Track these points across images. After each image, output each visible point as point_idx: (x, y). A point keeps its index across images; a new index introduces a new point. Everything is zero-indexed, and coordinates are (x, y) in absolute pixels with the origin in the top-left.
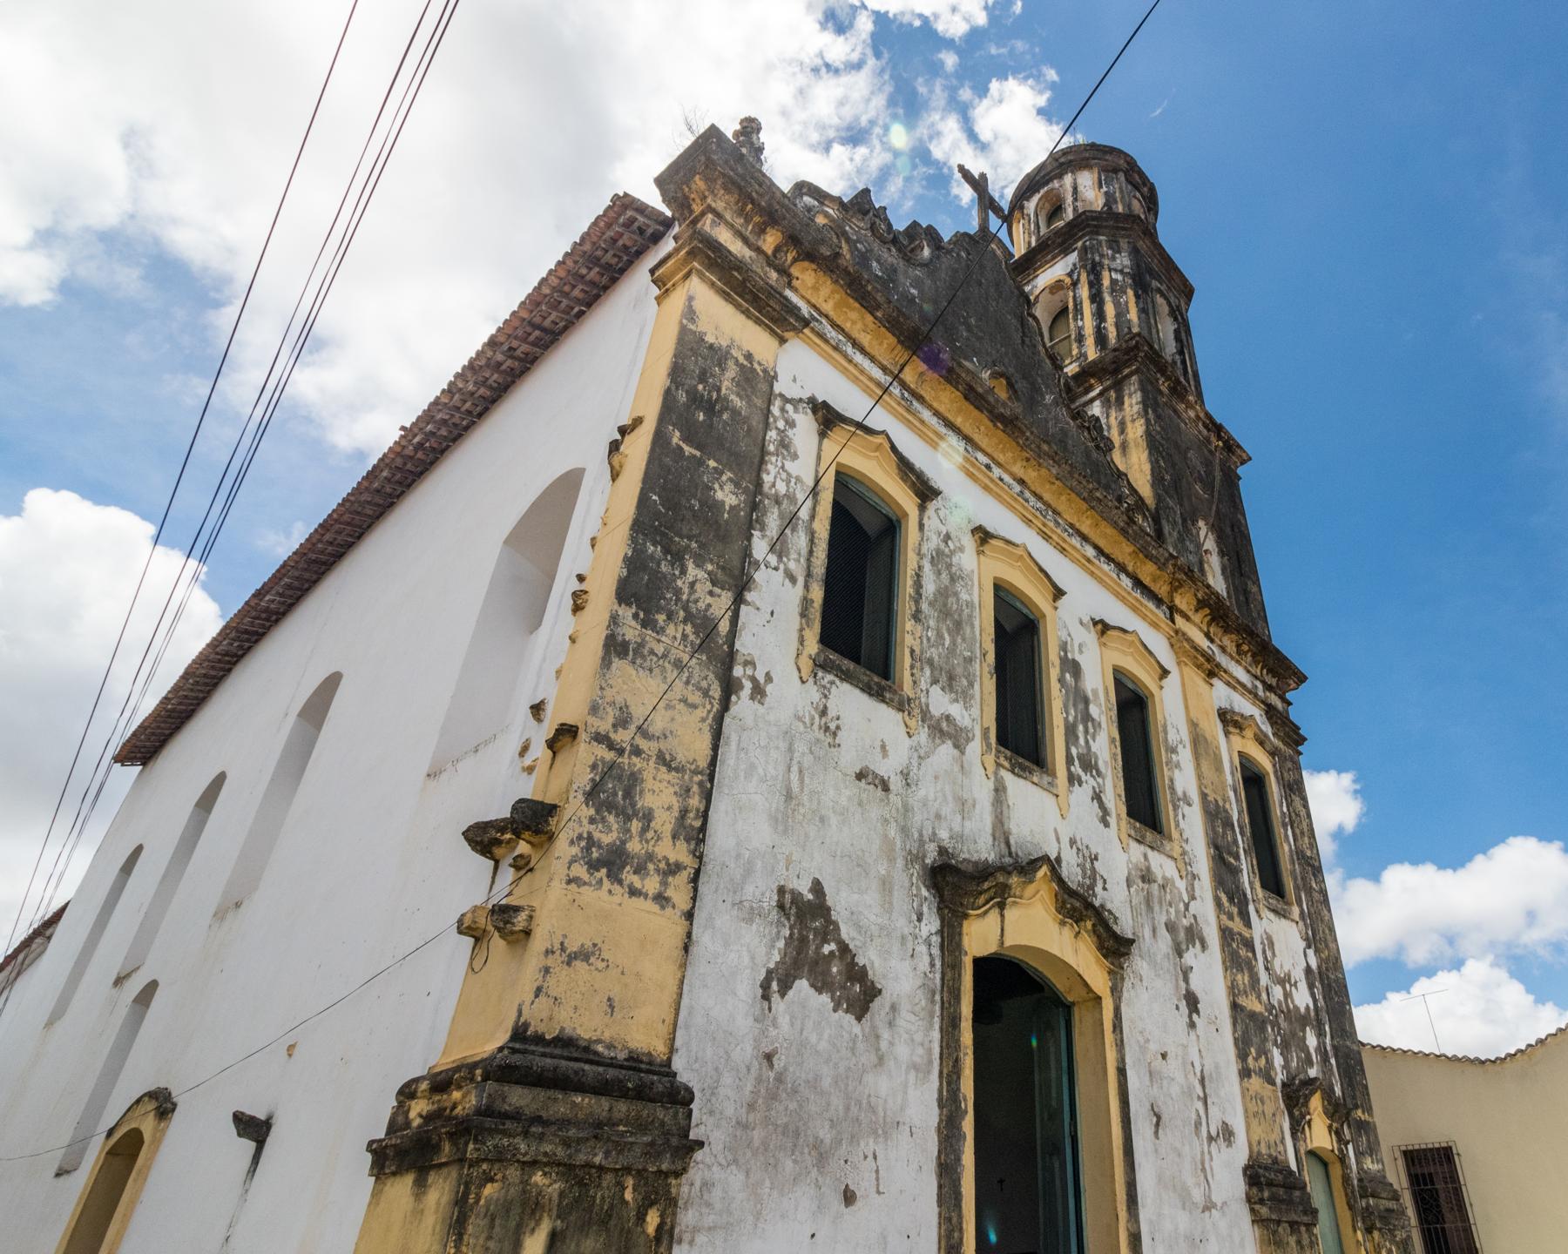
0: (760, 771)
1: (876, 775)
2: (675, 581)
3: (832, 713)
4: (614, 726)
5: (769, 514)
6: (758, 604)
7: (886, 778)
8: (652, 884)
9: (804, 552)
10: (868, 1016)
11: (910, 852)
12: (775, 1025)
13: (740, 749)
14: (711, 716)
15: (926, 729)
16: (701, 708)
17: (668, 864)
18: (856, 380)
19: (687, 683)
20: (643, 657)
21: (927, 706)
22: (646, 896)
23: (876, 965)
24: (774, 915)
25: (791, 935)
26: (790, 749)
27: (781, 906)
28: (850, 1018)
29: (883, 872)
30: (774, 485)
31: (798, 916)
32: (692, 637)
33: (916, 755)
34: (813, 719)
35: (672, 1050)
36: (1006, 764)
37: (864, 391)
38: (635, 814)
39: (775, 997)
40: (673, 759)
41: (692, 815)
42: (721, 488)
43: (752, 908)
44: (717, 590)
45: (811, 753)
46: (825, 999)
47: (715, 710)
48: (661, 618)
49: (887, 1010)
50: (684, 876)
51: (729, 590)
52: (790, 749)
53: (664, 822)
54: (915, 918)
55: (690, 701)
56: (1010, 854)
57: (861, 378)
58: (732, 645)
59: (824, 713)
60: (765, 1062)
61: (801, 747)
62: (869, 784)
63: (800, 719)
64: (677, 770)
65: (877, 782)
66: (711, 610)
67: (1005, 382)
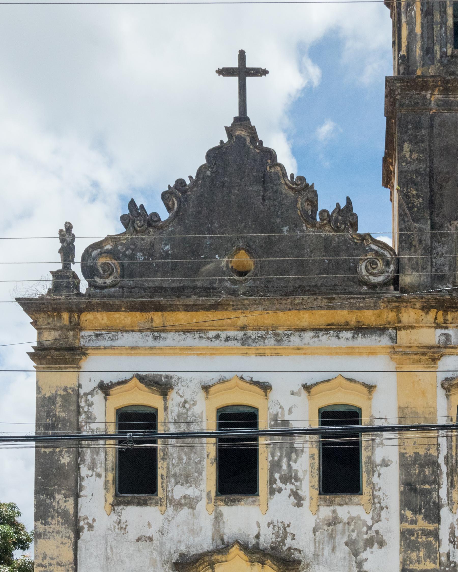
0: (95, 554)
1: (145, 537)
2: (52, 504)
4: (42, 560)
6: (86, 494)
7: (151, 536)
9: (103, 461)
11: (164, 560)
13: (86, 550)
15: (172, 507)
18: (121, 354)
19: (62, 537)
20: (46, 535)
21: (172, 496)
26: (106, 542)
32: (61, 521)
33: (166, 521)
34: (115, 527)
36: (222, 503)
40: (62, 563)
42: (63, 458)
44: (67, 499)
48: (49, 520)
55: (64, 542)
56: (223, 543)
59: (120, 522)
61: (110, 539)
63: (109, 529)
64: (63, 566)
65: (146, 539)
66: (66, 508)
67: (243, 251)
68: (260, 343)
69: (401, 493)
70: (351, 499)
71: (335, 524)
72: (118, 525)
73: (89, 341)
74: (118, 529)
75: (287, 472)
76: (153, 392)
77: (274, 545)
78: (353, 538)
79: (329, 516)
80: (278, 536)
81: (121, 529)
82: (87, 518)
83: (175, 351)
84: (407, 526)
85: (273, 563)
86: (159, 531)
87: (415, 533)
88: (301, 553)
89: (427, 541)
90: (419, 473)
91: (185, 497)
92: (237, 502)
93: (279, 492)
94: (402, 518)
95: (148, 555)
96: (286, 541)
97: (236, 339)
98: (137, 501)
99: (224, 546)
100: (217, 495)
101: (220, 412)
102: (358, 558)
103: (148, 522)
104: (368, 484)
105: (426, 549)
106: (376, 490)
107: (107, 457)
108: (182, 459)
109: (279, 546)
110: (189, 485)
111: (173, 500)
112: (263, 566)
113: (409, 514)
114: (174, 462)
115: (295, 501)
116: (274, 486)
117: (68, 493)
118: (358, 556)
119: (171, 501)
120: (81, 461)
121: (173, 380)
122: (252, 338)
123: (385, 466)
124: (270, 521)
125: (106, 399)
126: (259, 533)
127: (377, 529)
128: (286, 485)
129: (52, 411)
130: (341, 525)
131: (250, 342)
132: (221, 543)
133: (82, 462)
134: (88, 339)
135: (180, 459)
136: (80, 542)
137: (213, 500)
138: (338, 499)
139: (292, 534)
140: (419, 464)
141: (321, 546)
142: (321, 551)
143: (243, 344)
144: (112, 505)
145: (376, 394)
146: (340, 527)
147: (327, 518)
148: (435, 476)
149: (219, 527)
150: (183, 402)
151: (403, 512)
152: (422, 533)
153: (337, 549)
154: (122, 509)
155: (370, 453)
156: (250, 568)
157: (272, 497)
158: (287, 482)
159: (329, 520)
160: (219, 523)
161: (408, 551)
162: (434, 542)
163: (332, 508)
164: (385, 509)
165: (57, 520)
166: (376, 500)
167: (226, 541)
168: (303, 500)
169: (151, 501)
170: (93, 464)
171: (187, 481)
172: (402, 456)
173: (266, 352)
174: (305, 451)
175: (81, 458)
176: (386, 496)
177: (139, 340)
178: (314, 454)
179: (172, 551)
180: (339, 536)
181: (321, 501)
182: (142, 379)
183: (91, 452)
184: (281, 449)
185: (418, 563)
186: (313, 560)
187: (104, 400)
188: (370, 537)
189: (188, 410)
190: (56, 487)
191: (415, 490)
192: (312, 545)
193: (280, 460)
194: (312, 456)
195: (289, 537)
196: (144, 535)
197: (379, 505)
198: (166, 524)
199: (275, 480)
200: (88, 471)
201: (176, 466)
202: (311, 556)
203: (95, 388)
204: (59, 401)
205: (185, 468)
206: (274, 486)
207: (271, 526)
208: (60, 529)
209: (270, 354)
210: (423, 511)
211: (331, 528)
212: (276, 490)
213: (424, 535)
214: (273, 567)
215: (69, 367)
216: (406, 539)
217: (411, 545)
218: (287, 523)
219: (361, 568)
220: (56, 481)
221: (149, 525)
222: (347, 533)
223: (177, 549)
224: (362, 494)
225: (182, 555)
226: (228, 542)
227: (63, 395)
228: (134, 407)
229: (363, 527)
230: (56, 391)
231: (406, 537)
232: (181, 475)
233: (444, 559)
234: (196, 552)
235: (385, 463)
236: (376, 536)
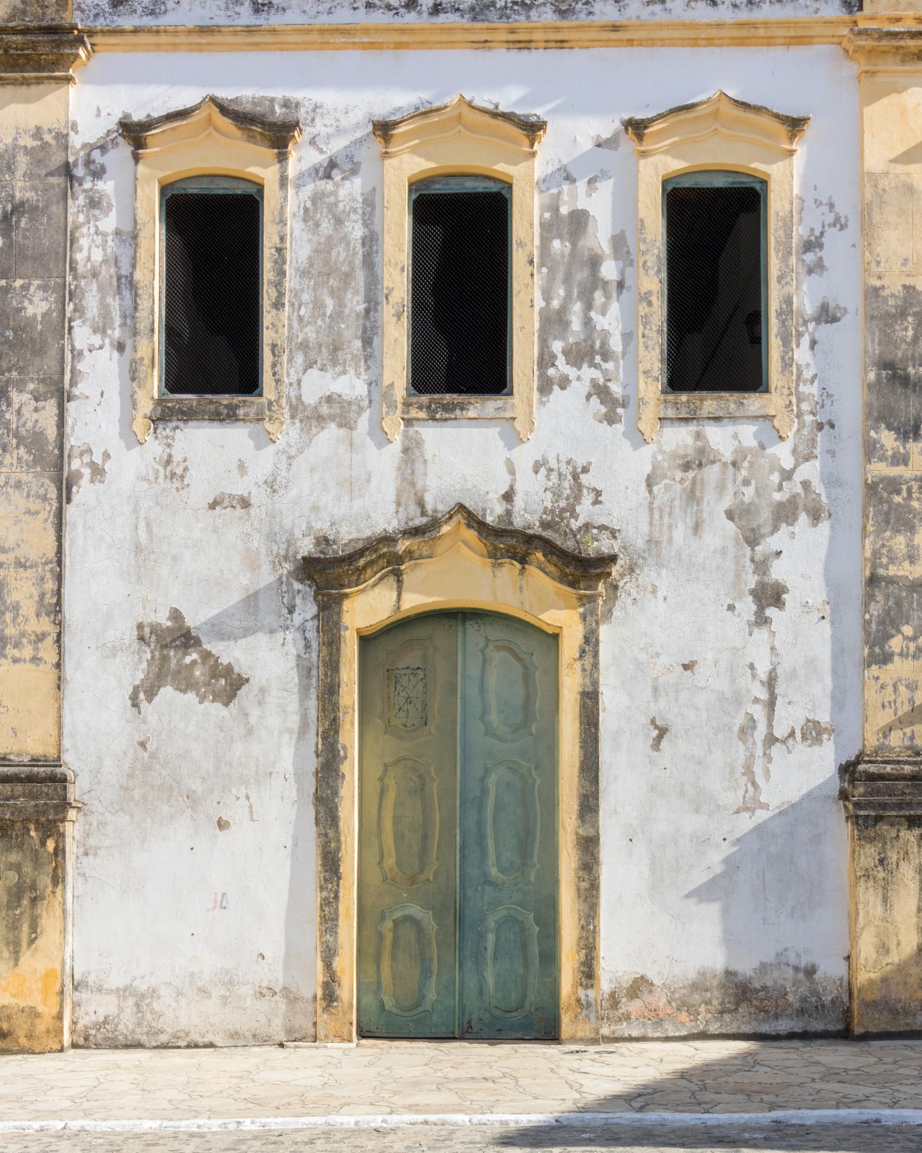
2: (3, 416)
3: (177, 457)
5: (86, 294)
7: (246, 495)
8: (27, 652)
10: (236, 701)
11: (278, 554)
12: (144, 722)
14: (52, 514)
15: (298, 424)
16: (42, 512)
17: (37, 636)
18: (175, 47)
19: (28, 496)
21: (299, 398)
22: (25, 661)
23: (242, 660)
24: (136, 645)
25: (153, 658)
27: (141, 638)
28: (218, 705)
29: (247, 582)
30: (89, 259)
31: (157, 641)
32: (26, 457)
33: (284, 457)
35: (60, 752)
36: (422, 415)
37: (191, 51)
38: (7, 609)
39: (144, 704)
40: (27, 560)
41: (48, 596)
42: (31, 302)
43: (114, 647)
44: (41, 404)
45: (157, 504)
46: (191, 696)
47: (54, 508)
49: (256, 692)
50: (50, 640)
51: (51, 398)
52: (136, 510)
53: (28, 608)
54: (286, 611)
55: (32, 510)
56: (423, 514)
57: (178, 40)
58: (61, 448)
59: (168, 462)
60: (139, 748)
62: (225, 508)
63: (144, 479)
64: (31, 567)
65: (234, 503)
66: (39, 425)
68: (517, 17)
70: (742, 403)
71: (700, 465)
72: (165, 467)
73: (97, 16)
74: (166, 477)
75: (583, 337)
76: (251, 138)
77: (549, 518)
78: (747, 500)
79: (686, 446)
80: (559, 496)
81: (171, 478)
82: (89, 451)
83: (308, 38)
84: (880, 469)
85: (549, 561)
86: (266, 482)
87: (904, 487)
88: (615, 537)
91: (329, 399)
93: (563, 388)
94: (871, 450)
95: (239, 542)
96: (578, 509)
97: (458, 10)
98: (212, 407)
99: (424, 520)
100: (409, 395)
101: (416, 190)
103: (240, 460)
106: (805, 382)
107: (139, 302)
108: (323, 306)
109: (562, 519)
110: (339, 369)
111: (300, 407)
112: (524, 568)
114: (302, 312)
115: (604, 410)
116: (551, 372)
117: (42, 389)
118: (758, 544)
119: (296, 408)
120: (75, 310)
121: (303, 110)
122: (498, 6)
123: (827, 322)
124: (540, 458)
125: (136, 158)
126: (512, 488)
127: (806, 478)
128: (579, 369)
129: (5, 187)
130: (717, 467)
131: (493, 15)
132: (418, 511)
133: (77, 314)
134: (94, 12)
135: (318, 305)
136: (71, 511)
137: (400, 406)
138: (710, 403)
139: (594, 489)
141: (666, 519)
142: (667, 533)
143: (474, 19)
144: (150, 418)
146: (712, 473)
147: (681, 452)
149: (413, 473)
150: (325, 165)
153: (706, 527)
154: (177, 428)
156: (491, 574)
157: (544, 399)
159: (686, 455)
160: (413, 462)
161: (885, 531)
163: (692, 428)
164: (827, 427)
165: (15, 456)
166: (805, 407)
167: (429, 507)
169: (246, 410)
170: (105, 318)
171: (334, 362)
174: (626, 285)
175: (75, 305)
176: (829, 396)
177: (218, 12)
178: (650, 293)
179: (298, 533)
180: (710, 496)
181: (666, 407)
182: (224, 109)
183: (101, 289)
184: (567, 280)
185: (911, 562)
187: (132, 162)
188: (788, 497)
189: (337, 185)
190: (15, 374)
192: (644, 517)
193: (564, 309)
195: (587, 499)
196: (228, 492)
198: (283, 466)
199: (554, 357)
200: (93, 337)
201: (308, 323)
202: (640, 543)
203: (109, 131)
204: (22, 163)
205: (330, 327)
206: (551, 372)
207: (543, 471)
208: (24, 478)
209: (543, 44)
211: (690, 474)
212: (556, 381)
214: (547, 570)
215: (48, 78)
216: (881, 501)
218: (580, 462)
219: (764, 574)
220: (14, 360)
221: (242, 467)
222: (731, 489)
223: (310, 528)
224: (767, 391)
225: (324, 541)
226: (435, 511)
227: (33, 148)
228: (205, 179)
229: (771, 471)
230: (16, 139)
231: (881, 498)
232: (320, 346)
234: (355, 535)
236: (803, 496)
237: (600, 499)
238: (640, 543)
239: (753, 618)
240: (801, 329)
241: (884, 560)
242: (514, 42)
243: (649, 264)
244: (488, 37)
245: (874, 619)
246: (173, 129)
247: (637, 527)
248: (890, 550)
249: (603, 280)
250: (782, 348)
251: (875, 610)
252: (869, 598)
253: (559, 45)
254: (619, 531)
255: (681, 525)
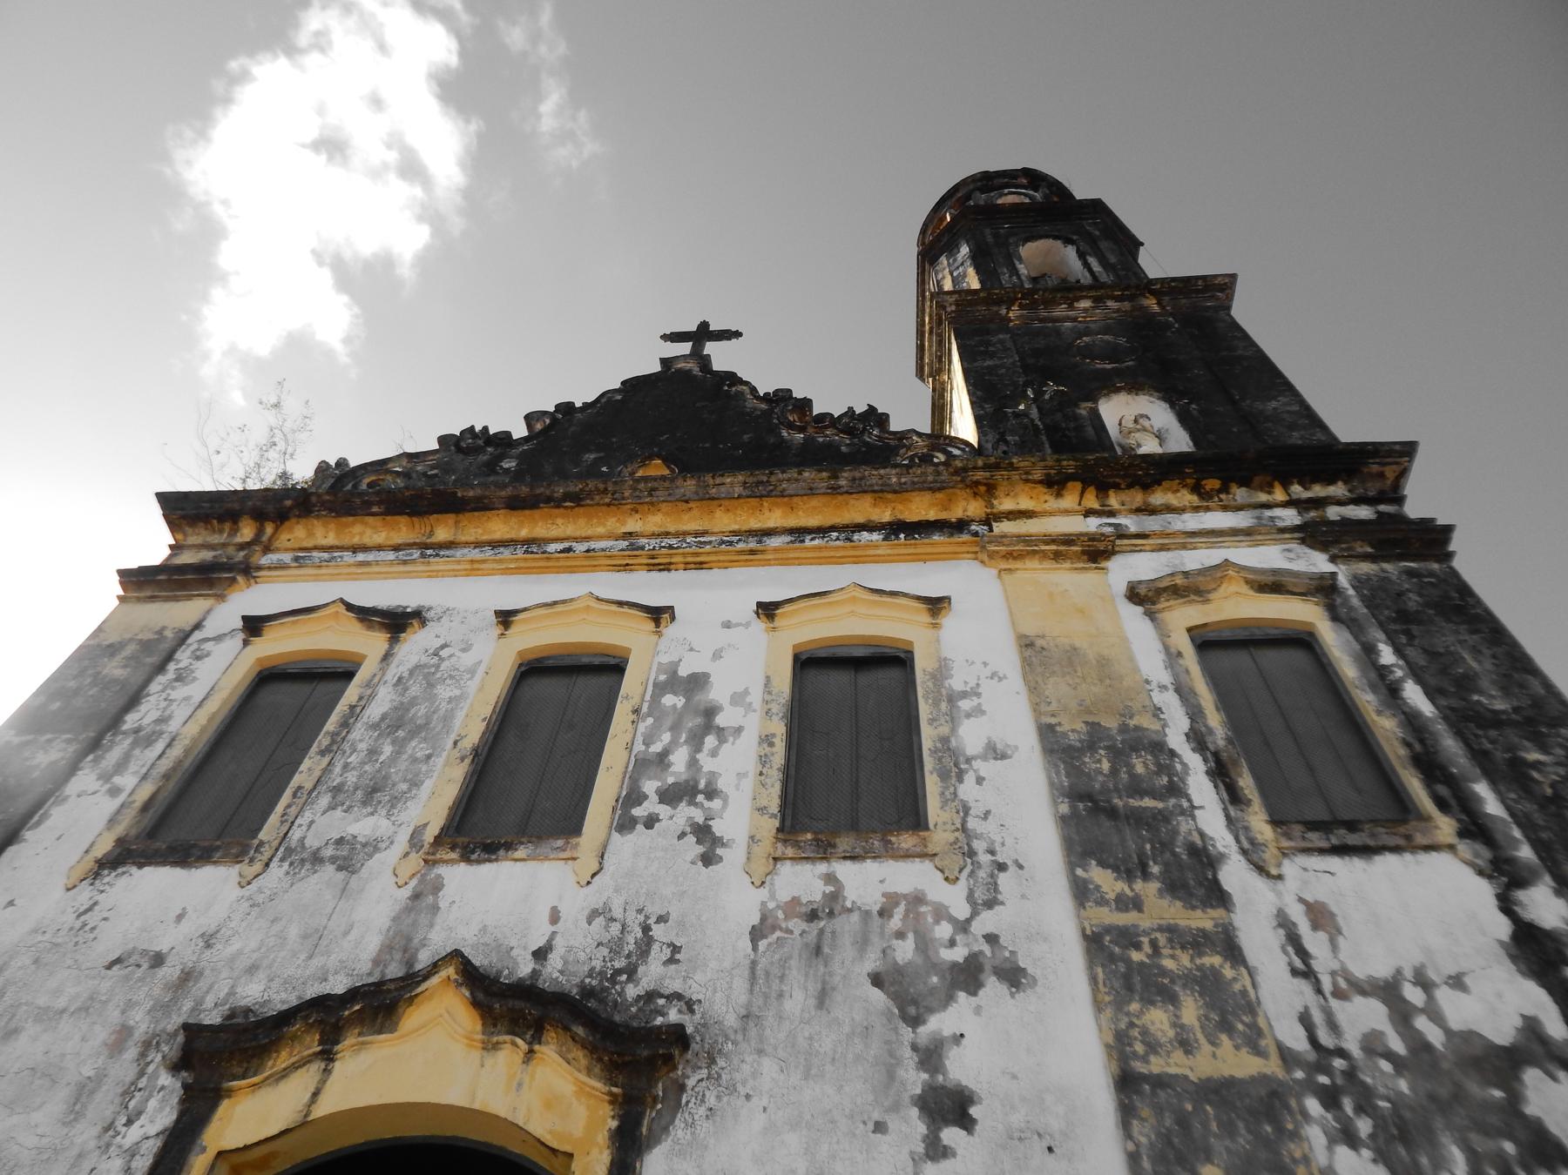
15: (286, 865)
69: (1063, 821)
71: (831, 914)
77: (594, 983)
86: (203, 935)
87: (1145, 940)
88: (692, 1011)
89: (1200, 968)
90: (1114, 771)
91: (340, 841)
92: (502, 852)
94: (1082, 893)
96: (641, 969)
102: (921, 1030)
104: (945, 803)
105: (1201, 995)
113: (1105, 880)
116: (637, 812)
123: (996, 759)
137: (426, 846)
140: (1106, 748)
141: (775, 985)
145: (949, 621)
148: (1170, 776)
151: (1079, 872)
152: (1170, 940)
155: (945, 730)
158: (681, 800)
161: (1129, 1002)
162: (1228, 973)
164: (1012, 869)
168: (723, 845)
172: (1047, 733)
173: (673, 561)
178: (774, 735)
182: (350, 607)
186: (740, 1037)
191: (1112, 813)
192: (740, 985)
194: (767, 740)
195: (658, 954)
197: (989, 857)
202: (731, 1020)
207: (600, 921)
209: (682, 566)
210: (1155, 869)
213: (1183, 948)
216: (1112, 958)
217: (1137, 979)
218: (655, 910)
222: (877, 944)
232: (356, 789)
233: (1296, 1040)
235: (995, 752)
237: (677, 956)
238: (731, 1020)
239: (920, 1148)
240: (962, 766)
241: (1139, 1048)
242: (654, 565)
243: (774, 711)
244: (630, 562)
245: (1143, 1151)
246: (294, 622)
247: (728, 997)
248: (1145, 1032)
249: (718, 727)
250: (940, 784)
251: (1143, 1133)
252: (1126, 1113)
253: (698, 566)
254: (700, 1001)
255: (799, 995)
